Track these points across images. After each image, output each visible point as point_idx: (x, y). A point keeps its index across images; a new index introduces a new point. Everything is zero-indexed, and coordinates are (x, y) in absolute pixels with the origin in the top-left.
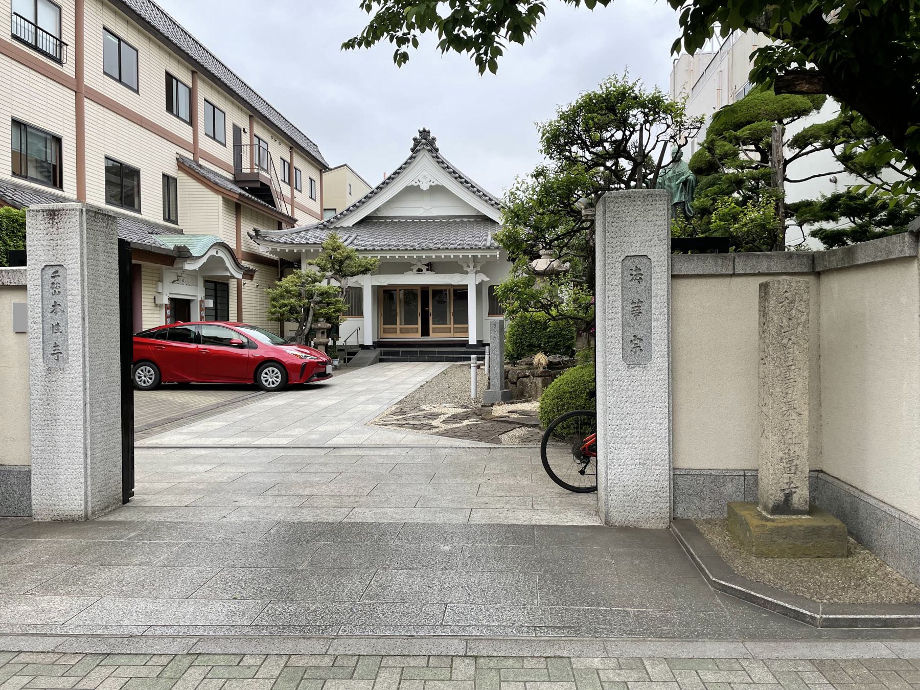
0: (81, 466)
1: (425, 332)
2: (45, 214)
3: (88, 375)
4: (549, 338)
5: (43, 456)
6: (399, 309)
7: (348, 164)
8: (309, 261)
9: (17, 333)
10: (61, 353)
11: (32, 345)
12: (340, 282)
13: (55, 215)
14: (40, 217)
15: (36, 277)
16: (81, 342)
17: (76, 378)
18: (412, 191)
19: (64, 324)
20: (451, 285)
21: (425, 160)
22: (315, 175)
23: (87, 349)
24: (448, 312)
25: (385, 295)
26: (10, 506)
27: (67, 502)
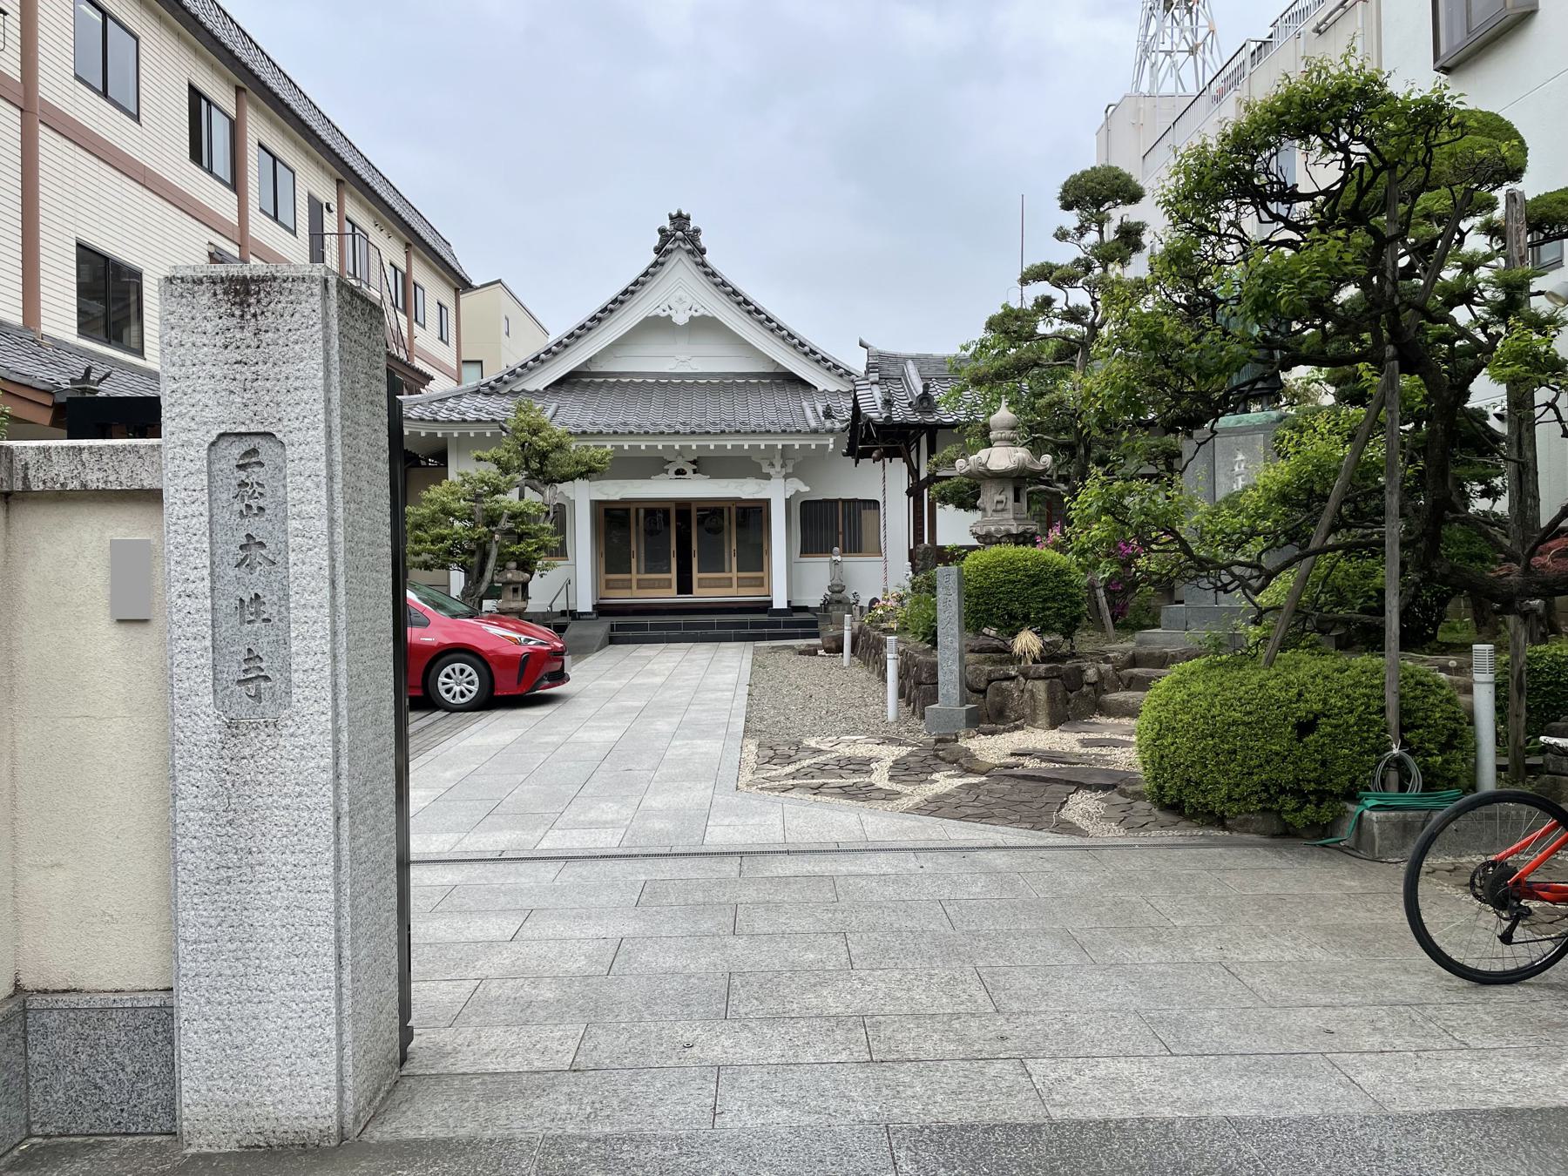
0: (327, 992)
1: (685, 586)
2: (219, 289)
3: (344, 737)
4: (1045, 601)
5: (215, 967)
6: (637, 545)
7: (504, 281)
8: (479, 453)
9: (120, 621)
10: (266, 678)
11: (180, 658)
12: (542, 493)
13: (248, 293)
14: (205, 299)
15: (193, 467)
16: (327, 648)
17: (313, 747)
18: (657, 325)
19: (275, 598)
20: (739, 500)
21: (680, 269)
22: (448, 298)
23: (343, 666)
24: (726, 550)
25: (611, 518)
26: (106, 1106)
27: (288, 1095)
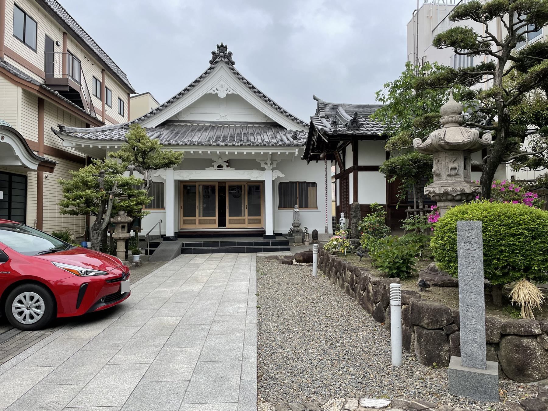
1: (222, 223)
6: (199, 204)
7: (150, 92)
12: (143, 174)
20: (248, 181)
21: (222, 71)
22: (124, 97)
